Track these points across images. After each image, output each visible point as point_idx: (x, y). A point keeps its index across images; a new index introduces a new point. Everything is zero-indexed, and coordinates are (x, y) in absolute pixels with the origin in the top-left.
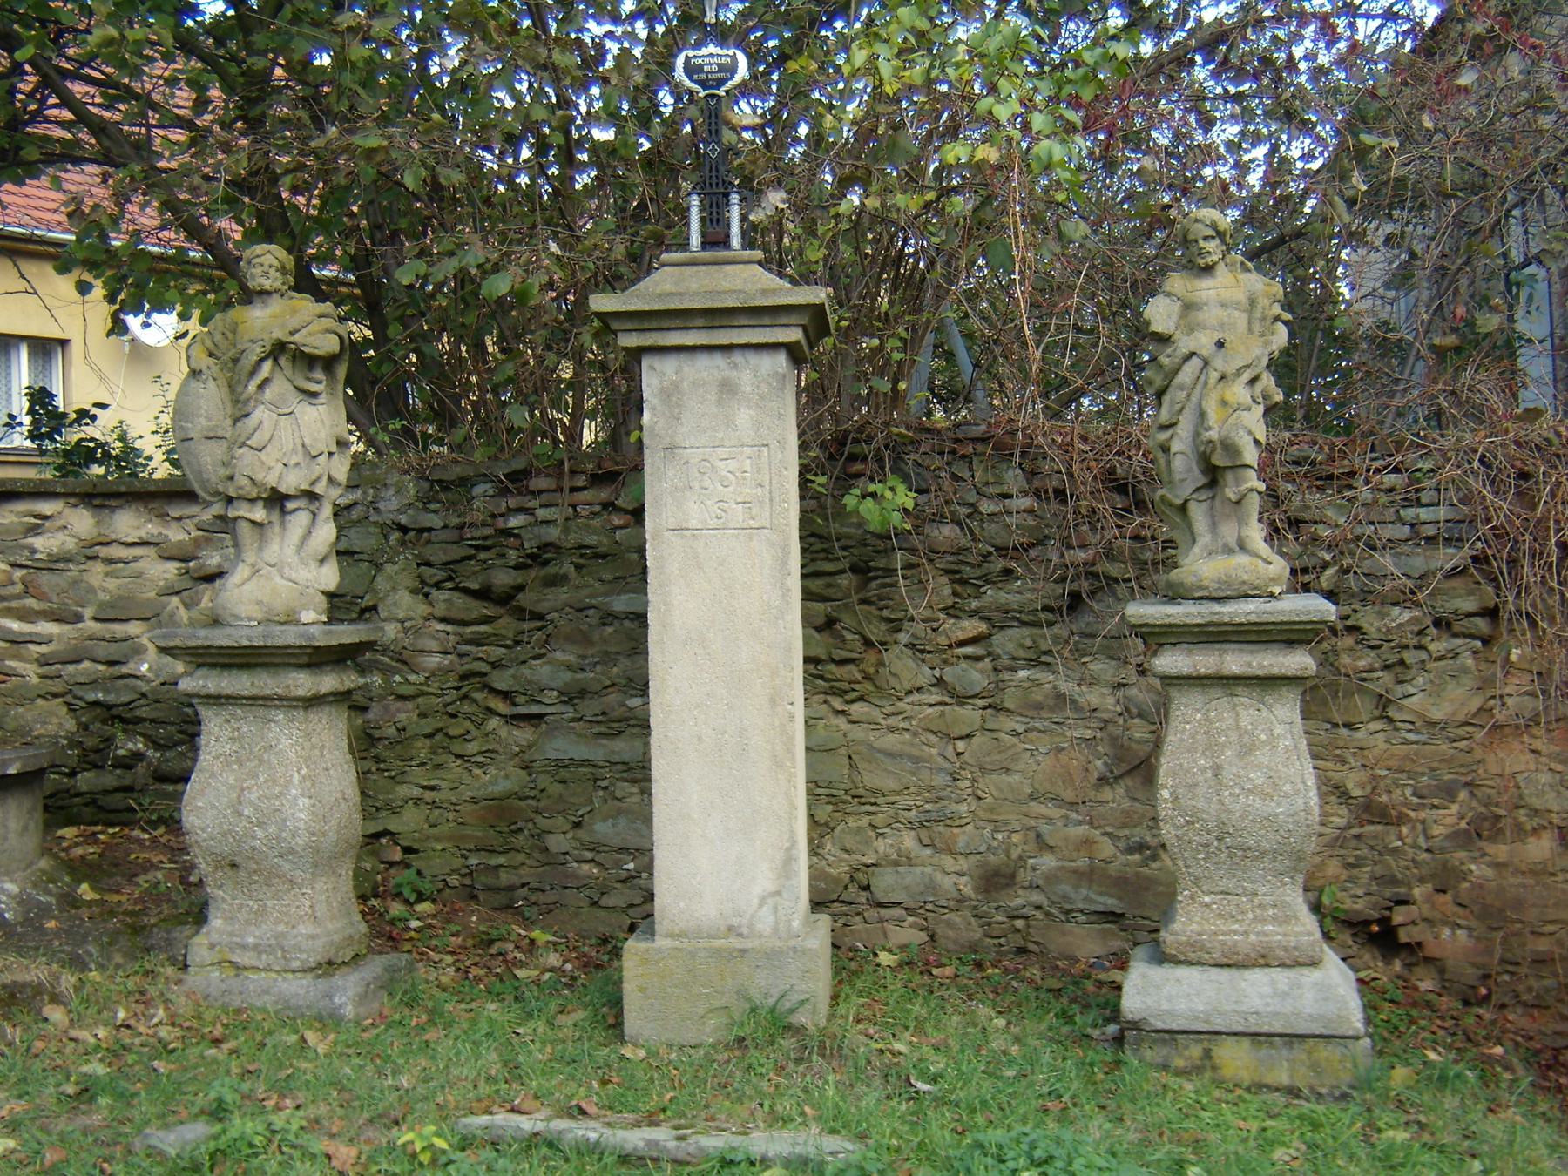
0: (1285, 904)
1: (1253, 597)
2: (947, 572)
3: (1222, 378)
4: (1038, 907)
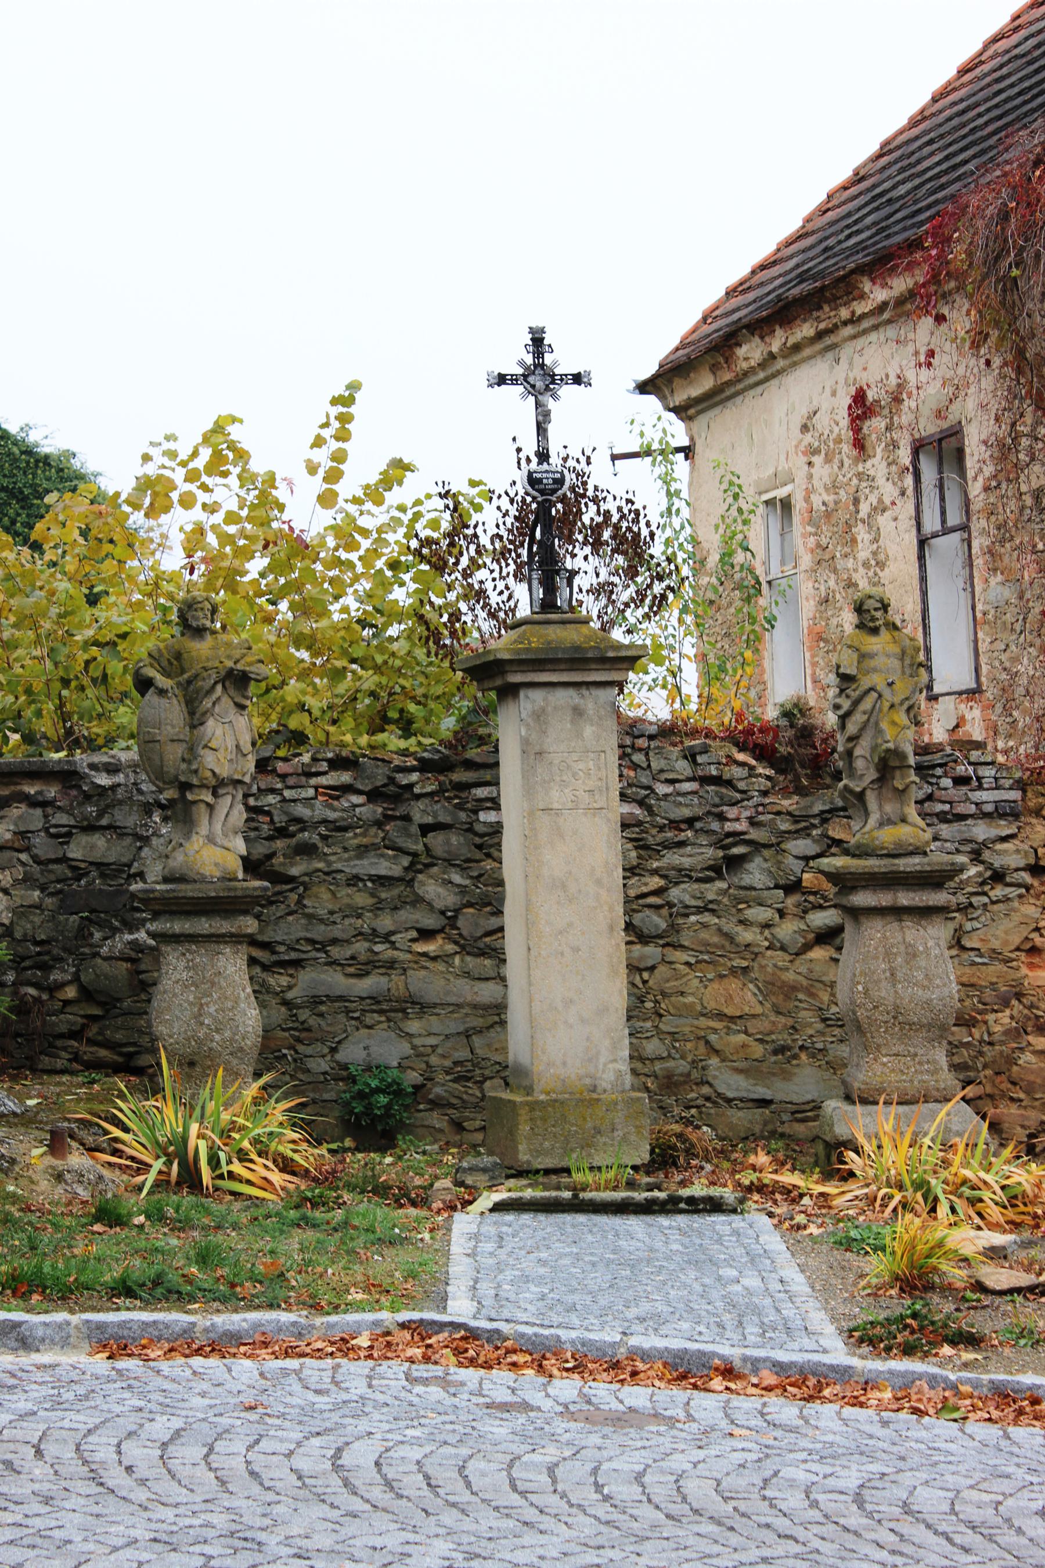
0: (935, 1062)
2: (631, 840)
3: (892, 706)
4: (708, 1099)
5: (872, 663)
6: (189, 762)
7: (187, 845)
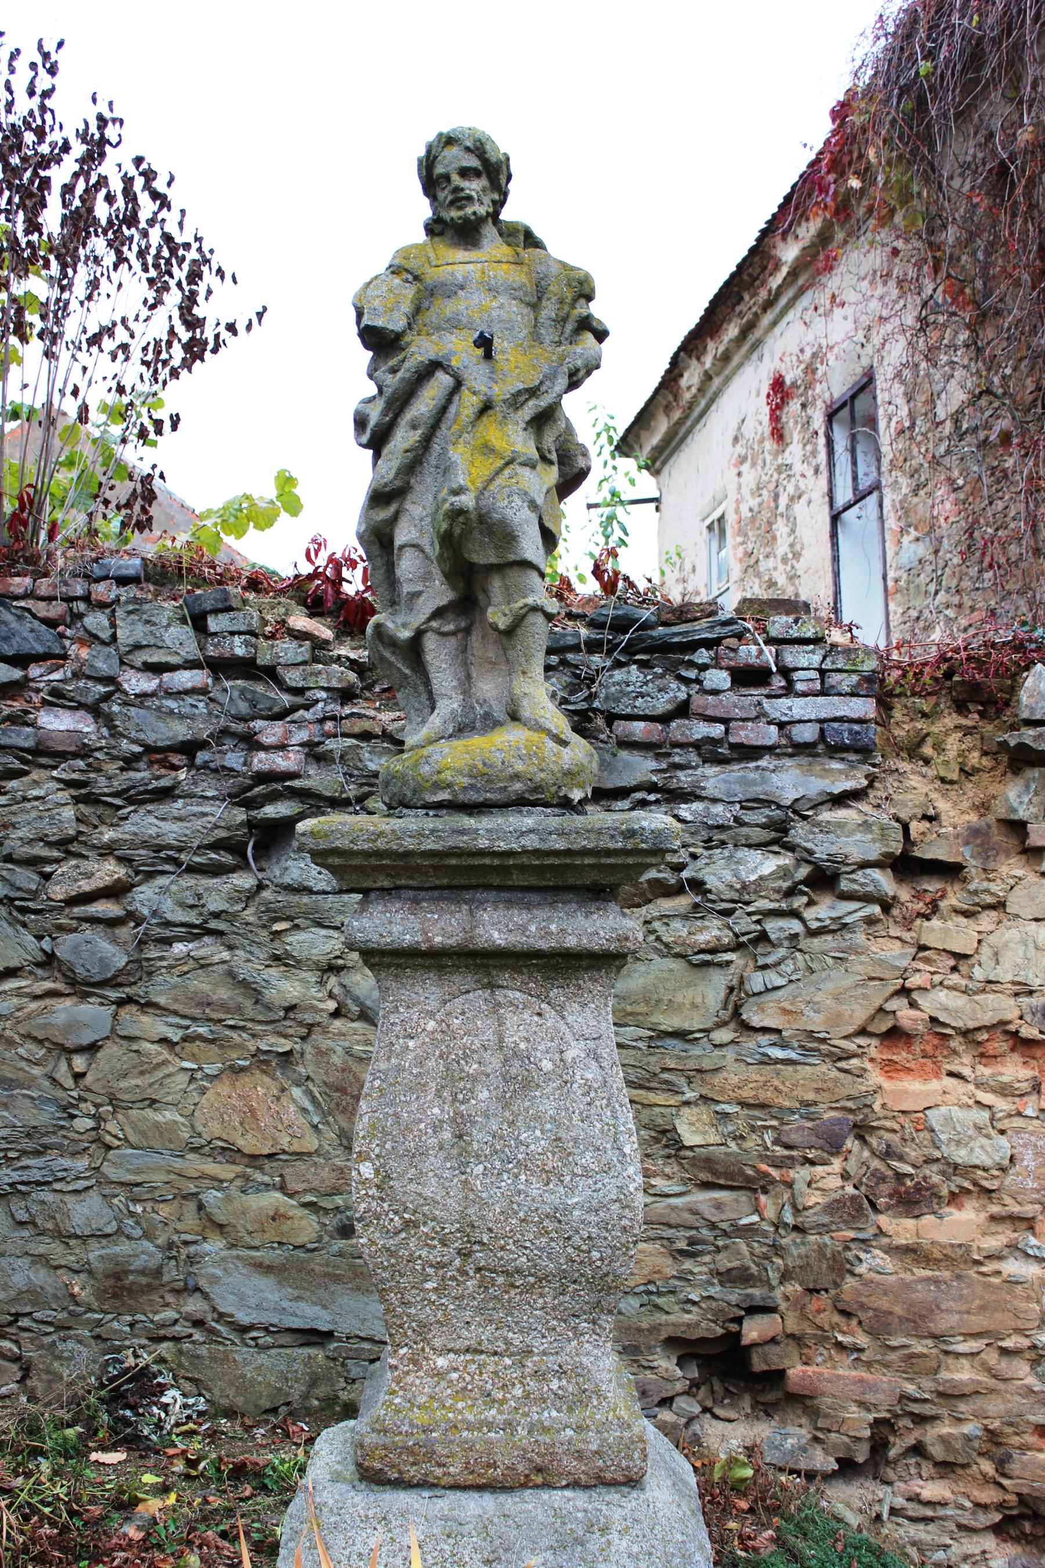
0: (579, 1372)
1: (534, 804)
2: (69, 784)
3: (486, 408)
4: (199, 1323)
5: (449, 308)
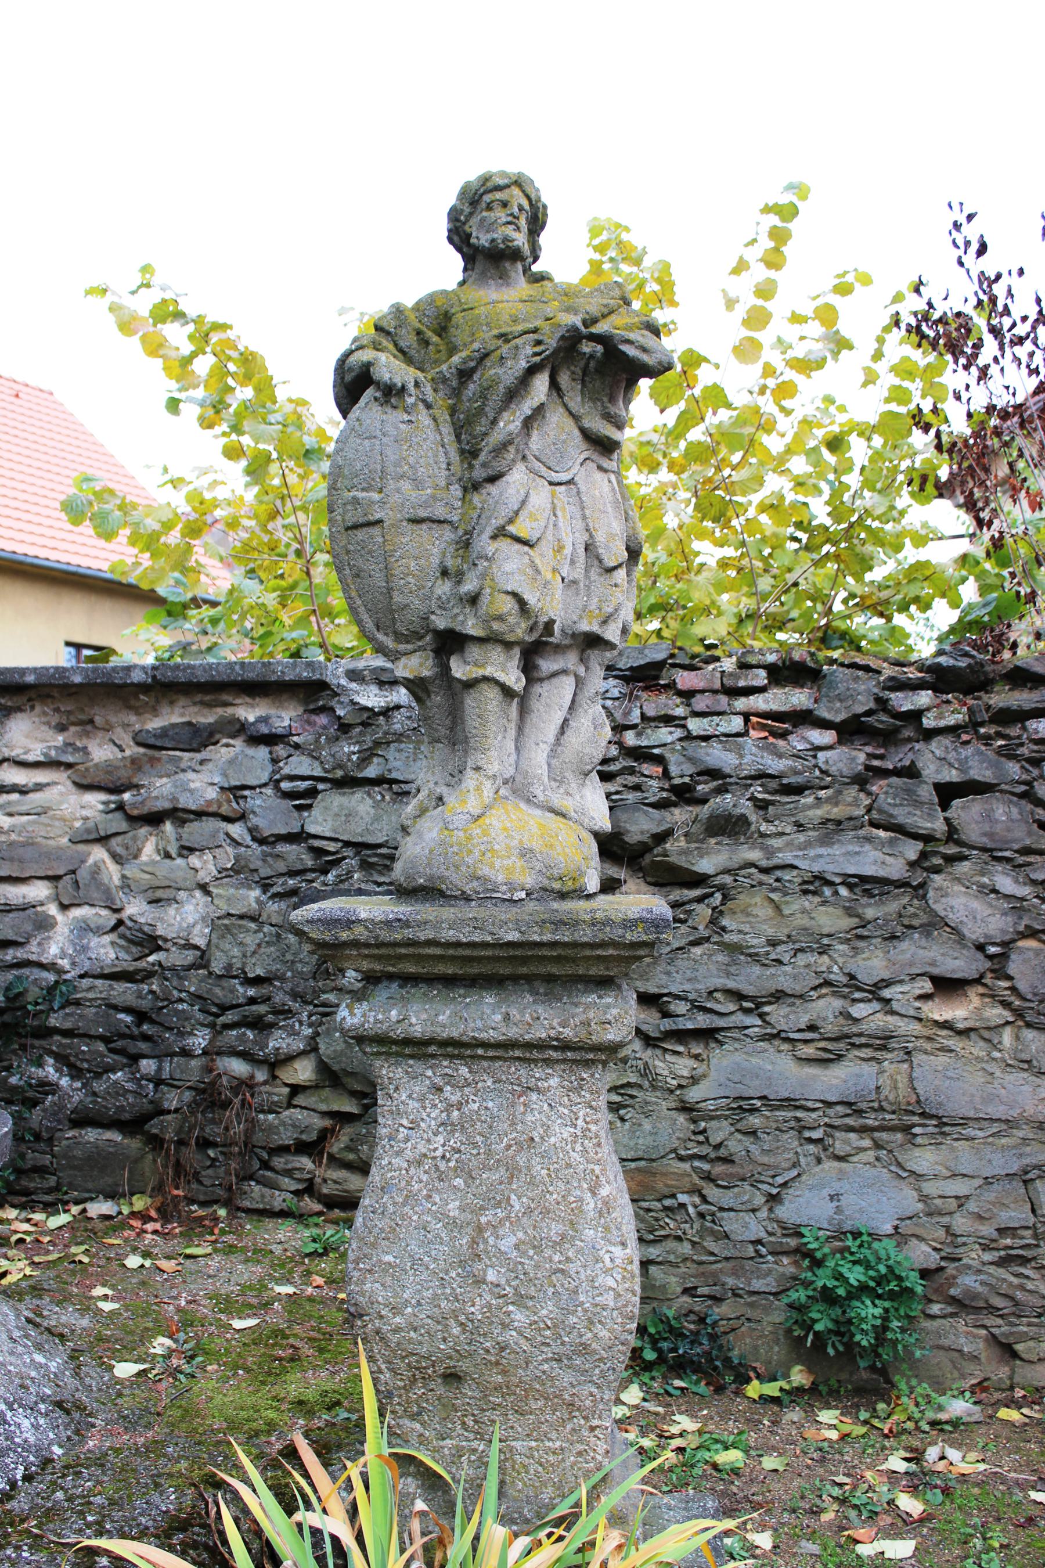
6: (459, 577)
7: (451, 800)
